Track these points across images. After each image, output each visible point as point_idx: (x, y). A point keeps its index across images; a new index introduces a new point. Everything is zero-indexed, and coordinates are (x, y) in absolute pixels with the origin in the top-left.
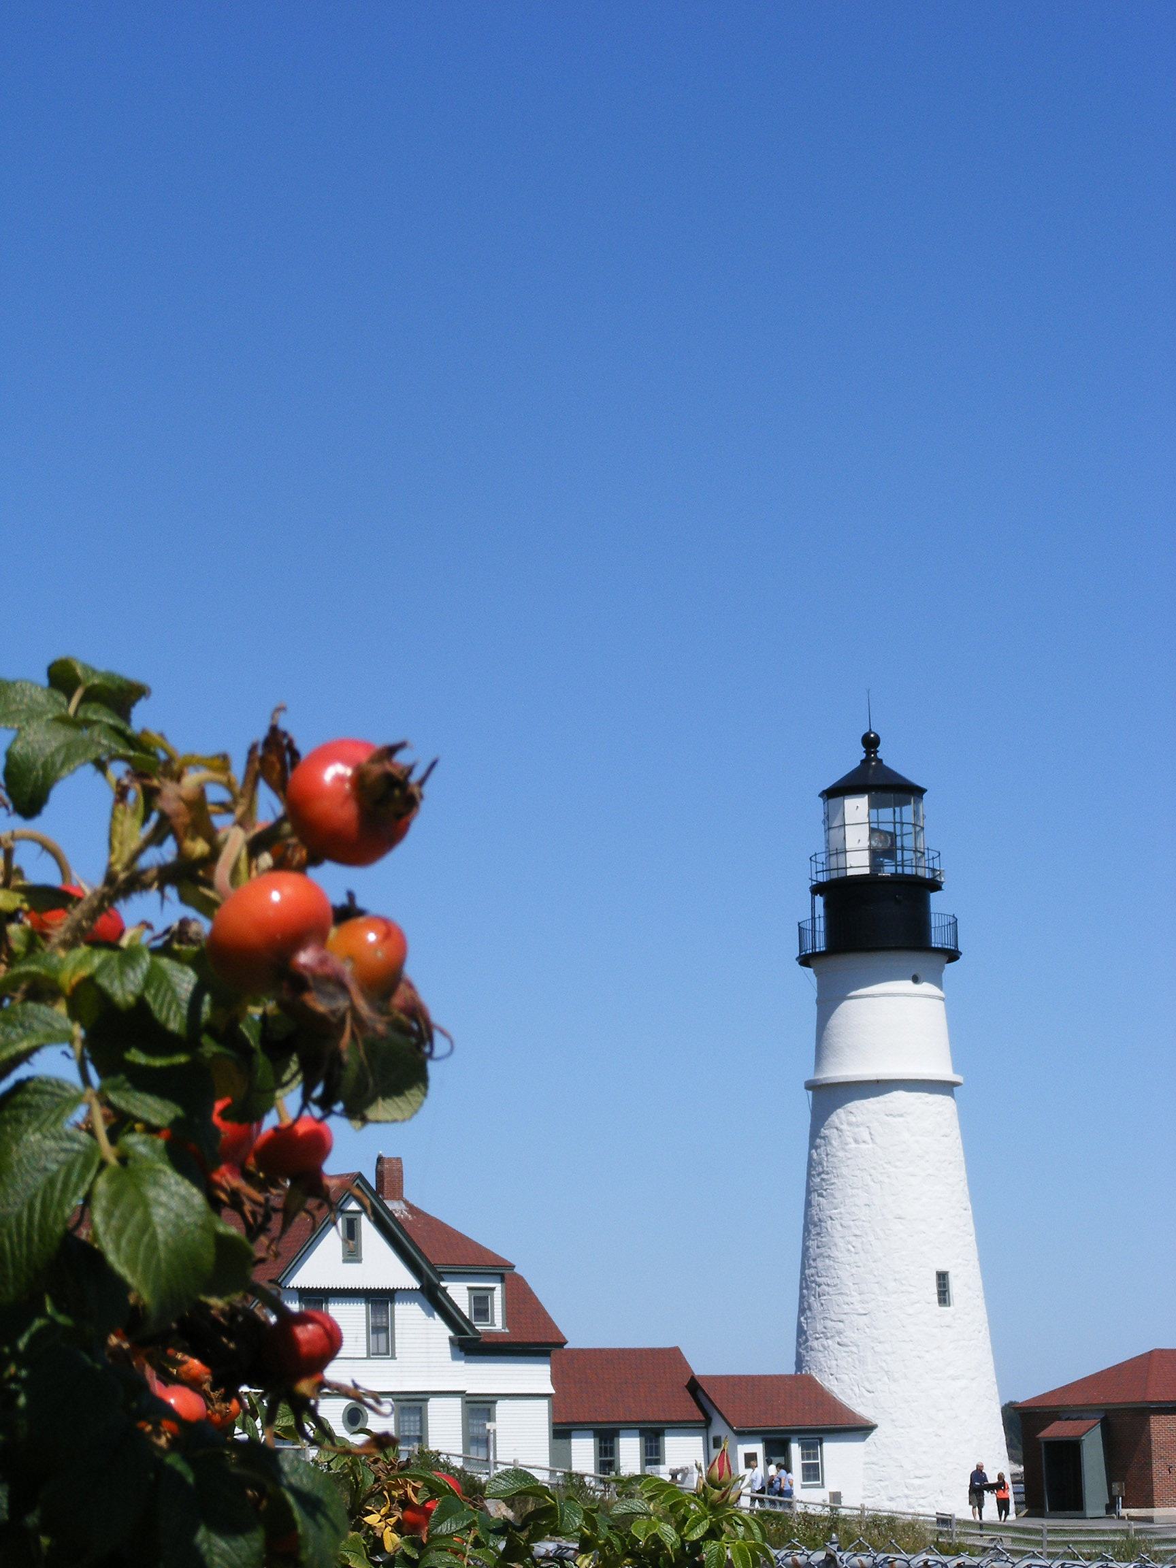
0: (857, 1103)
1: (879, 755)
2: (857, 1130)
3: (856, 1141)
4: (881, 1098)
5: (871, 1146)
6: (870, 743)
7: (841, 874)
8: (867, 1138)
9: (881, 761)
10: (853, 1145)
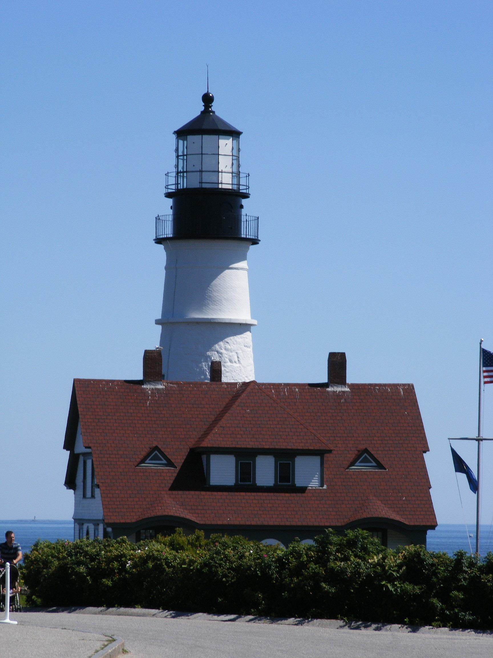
0: (232, 338)
1: (213, 109)
2: (231, 354)
3: (231, 361)
4: (242, 335)
5: (238, 365)
6: (208, 99)
7: (215, 186)
8: (236, 360)
9: (214, 112)
10: (229, 364)
